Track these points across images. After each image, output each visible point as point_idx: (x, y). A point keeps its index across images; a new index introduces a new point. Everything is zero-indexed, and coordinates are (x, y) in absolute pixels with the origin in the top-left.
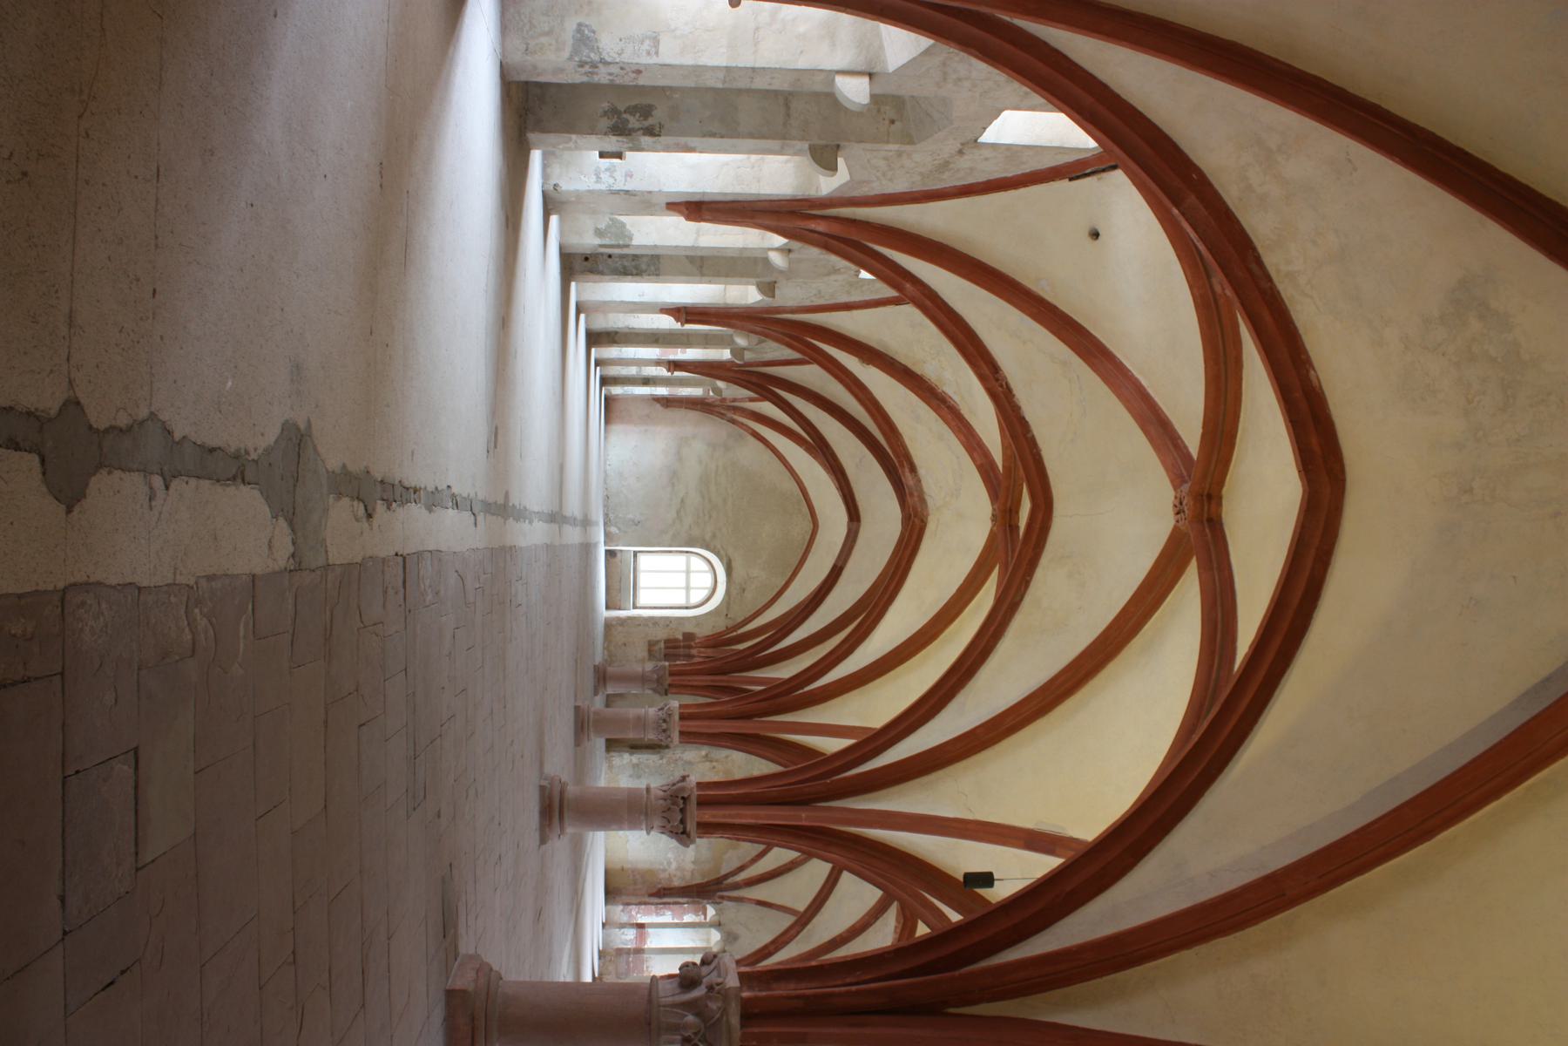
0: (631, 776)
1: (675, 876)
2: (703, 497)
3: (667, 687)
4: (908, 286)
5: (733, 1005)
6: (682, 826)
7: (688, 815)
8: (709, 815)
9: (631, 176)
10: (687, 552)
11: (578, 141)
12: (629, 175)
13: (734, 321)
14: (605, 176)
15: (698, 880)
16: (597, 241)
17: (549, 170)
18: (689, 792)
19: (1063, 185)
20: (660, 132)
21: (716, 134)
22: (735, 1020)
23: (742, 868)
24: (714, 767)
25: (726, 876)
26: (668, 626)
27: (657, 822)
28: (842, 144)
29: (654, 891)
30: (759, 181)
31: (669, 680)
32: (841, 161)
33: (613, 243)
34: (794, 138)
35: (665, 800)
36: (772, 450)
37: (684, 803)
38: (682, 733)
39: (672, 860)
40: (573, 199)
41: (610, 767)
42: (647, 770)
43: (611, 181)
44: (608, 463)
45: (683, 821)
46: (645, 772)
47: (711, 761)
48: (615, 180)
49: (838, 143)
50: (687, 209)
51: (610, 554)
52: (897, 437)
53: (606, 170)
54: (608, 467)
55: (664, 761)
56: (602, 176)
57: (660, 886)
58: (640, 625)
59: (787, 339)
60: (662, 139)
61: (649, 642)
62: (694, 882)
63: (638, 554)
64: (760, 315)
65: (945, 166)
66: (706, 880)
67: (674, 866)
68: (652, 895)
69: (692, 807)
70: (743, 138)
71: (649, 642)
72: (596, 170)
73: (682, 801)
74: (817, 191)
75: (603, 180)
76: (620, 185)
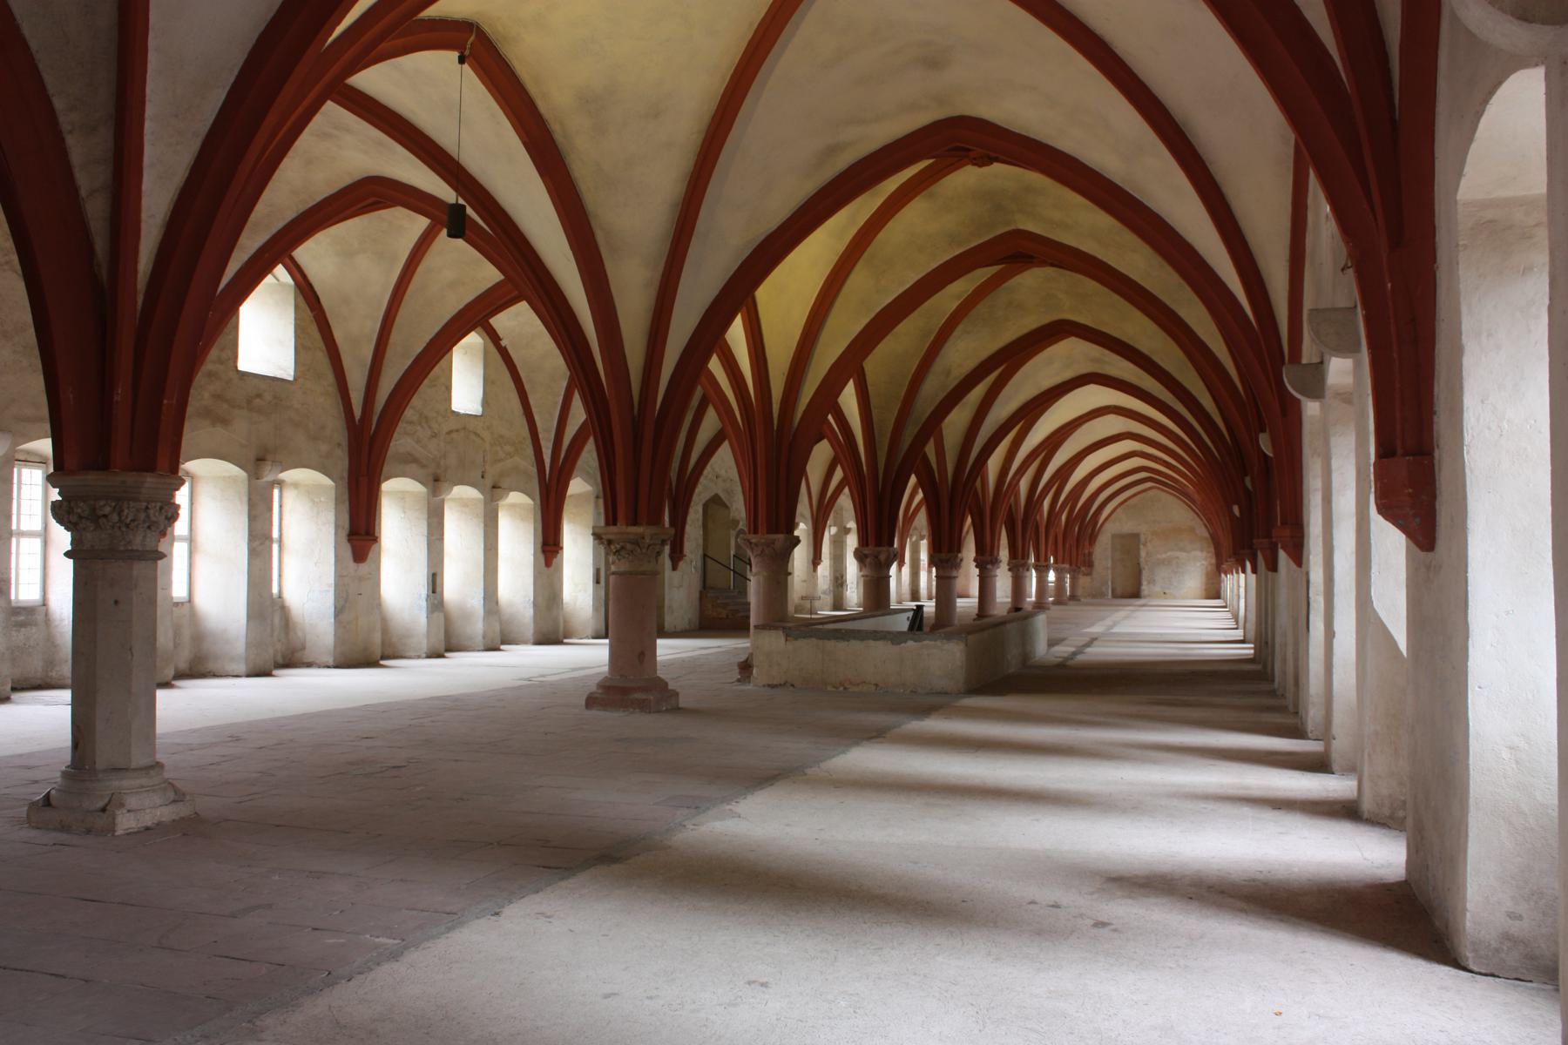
8: (1042, 558)
15: (1212, 549)
27: (1045, 574)
31: (1074, 567)
32: (848, 526)
38: (1063, 563)
41: (1149, 596)
67: (1203, 562)
69: (1039, 564)
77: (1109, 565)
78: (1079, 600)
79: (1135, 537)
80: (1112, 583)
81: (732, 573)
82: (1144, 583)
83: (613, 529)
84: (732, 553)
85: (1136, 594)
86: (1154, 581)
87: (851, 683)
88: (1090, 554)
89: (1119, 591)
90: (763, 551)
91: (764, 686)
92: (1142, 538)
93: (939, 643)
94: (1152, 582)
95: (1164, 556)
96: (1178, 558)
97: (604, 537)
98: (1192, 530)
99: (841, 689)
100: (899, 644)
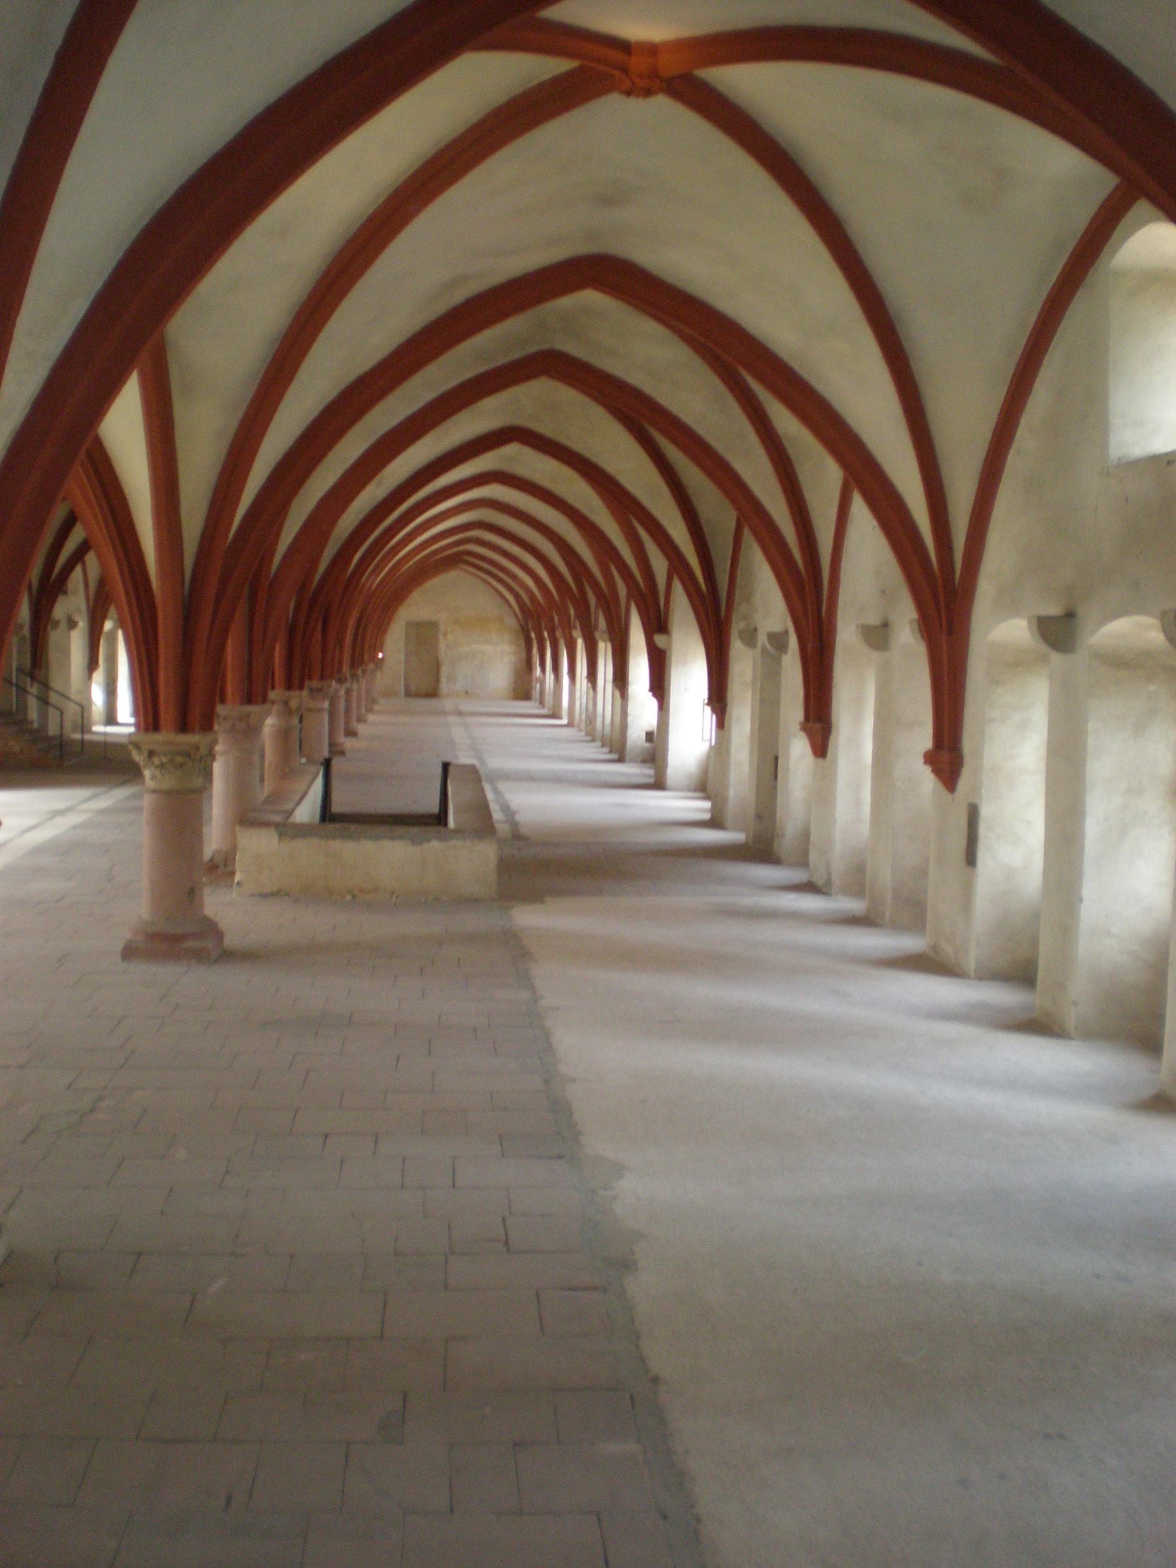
23: (516, 615)
41: (449, 695)
79: (433, 626)
81: (14, 689)
82: (444, 680)
83: (158, 737)
84: (14, 665)
85: (433, 693)
87: (361, 891)
90: (233, 728)
91: (252, 895)
92: (442, 628)
93: (468, 843)
97: (144, 747)
99: (349, 897)
100: (421, 844)
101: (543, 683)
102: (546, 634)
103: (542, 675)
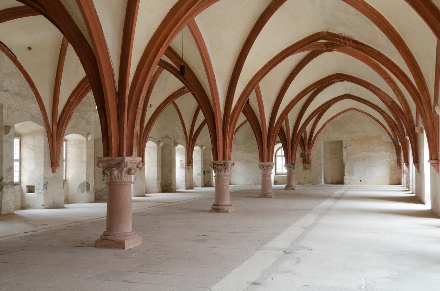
0: (353, 176)
1: (392, 159)
2: (254, 152)
3: (292, 165)
4: (71, 100)
5: (101, 159)
6: (223, 165)
7: (219, 163)
9: (39, 184)
10: (275, 156)
11: (6, 200)
12: (39, 184)
13: (142, 148)
14: (40, 191)
15: (394, 150)
16: (86, 192)
17: (38, 207)
18: (212, 163)
19: (19, 59)
20: (1, 177)
21: (2, 161)
22: (106, 158)
23: (389, 134)
24: (350, 145)
25: (392, 139)
26: (298, 163)
27: (223, 173)
28: (4, 125)
29: (399, 166)
30: (40, 146)
31: (290, 164)
33: (86, 187)
34: (2, 139)
35: (216, 171)
36: (238, 129)
37: (215, 165)
38: (268, 161)
39: (386, 160)
40: (51, 200)
41: (350, 183)
42: (351, 170)
43: (41, 189)
44: (244, 184)
45: (221, 165)
46: (352, 170)
47: (347, 146)
48: (41, 188)
49: (4, 128)
50: (53, 167)
51: (275, 183)
52: (175, 93)
53: (38, 191)
54: (245, 184)
55: (347, 163)
56: (39, 192)
57: (397, 164)
58: (298, 173)
59: (147, 131)
60: (3, 176)
61: (304, 169)
62: (395, 151)
63: (276, 173)
64: (139, 140)
65: (18, 95)
66: (394, 147)
68: (400, 168)
69: (216, 162)
70: (2, 154)
71: (304, 169)
72: (38, 194)
73: (214, 165)
74: (43, 129)
75: (41, 191)
76: (42, 187)
77: (322, 162)
78: (227, 212)
79: (340, 143)
80: (324, 174)
82: (346, 174)
85: (341, 182)
86: (353, 172)
88: (309, 155)
89: (329, 180)
92: (344, 144)
94: (352, 173)
95: (360, 155)
96: (369, 156)
98: (380, 137)
101: (408, 174)
102: (408, 138)
103: (407, 168)
